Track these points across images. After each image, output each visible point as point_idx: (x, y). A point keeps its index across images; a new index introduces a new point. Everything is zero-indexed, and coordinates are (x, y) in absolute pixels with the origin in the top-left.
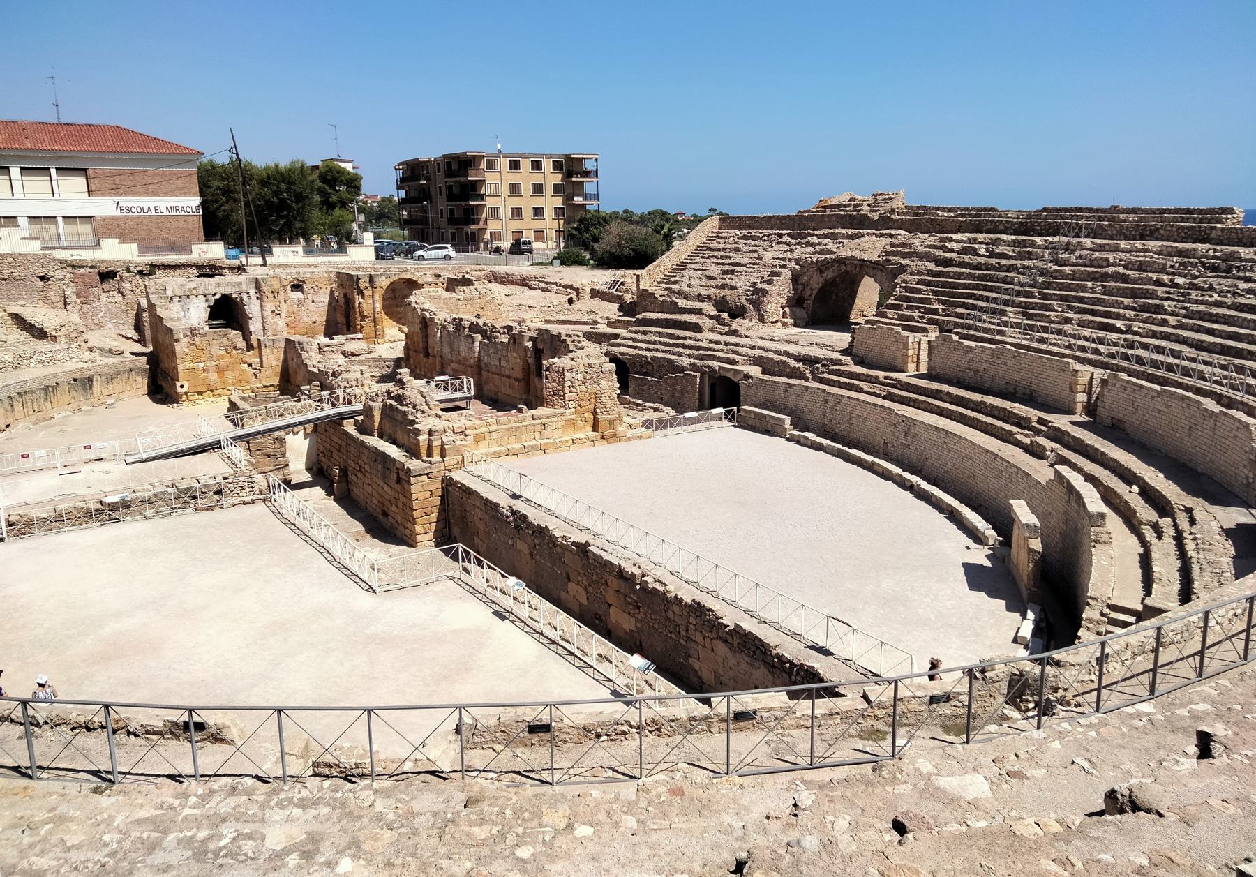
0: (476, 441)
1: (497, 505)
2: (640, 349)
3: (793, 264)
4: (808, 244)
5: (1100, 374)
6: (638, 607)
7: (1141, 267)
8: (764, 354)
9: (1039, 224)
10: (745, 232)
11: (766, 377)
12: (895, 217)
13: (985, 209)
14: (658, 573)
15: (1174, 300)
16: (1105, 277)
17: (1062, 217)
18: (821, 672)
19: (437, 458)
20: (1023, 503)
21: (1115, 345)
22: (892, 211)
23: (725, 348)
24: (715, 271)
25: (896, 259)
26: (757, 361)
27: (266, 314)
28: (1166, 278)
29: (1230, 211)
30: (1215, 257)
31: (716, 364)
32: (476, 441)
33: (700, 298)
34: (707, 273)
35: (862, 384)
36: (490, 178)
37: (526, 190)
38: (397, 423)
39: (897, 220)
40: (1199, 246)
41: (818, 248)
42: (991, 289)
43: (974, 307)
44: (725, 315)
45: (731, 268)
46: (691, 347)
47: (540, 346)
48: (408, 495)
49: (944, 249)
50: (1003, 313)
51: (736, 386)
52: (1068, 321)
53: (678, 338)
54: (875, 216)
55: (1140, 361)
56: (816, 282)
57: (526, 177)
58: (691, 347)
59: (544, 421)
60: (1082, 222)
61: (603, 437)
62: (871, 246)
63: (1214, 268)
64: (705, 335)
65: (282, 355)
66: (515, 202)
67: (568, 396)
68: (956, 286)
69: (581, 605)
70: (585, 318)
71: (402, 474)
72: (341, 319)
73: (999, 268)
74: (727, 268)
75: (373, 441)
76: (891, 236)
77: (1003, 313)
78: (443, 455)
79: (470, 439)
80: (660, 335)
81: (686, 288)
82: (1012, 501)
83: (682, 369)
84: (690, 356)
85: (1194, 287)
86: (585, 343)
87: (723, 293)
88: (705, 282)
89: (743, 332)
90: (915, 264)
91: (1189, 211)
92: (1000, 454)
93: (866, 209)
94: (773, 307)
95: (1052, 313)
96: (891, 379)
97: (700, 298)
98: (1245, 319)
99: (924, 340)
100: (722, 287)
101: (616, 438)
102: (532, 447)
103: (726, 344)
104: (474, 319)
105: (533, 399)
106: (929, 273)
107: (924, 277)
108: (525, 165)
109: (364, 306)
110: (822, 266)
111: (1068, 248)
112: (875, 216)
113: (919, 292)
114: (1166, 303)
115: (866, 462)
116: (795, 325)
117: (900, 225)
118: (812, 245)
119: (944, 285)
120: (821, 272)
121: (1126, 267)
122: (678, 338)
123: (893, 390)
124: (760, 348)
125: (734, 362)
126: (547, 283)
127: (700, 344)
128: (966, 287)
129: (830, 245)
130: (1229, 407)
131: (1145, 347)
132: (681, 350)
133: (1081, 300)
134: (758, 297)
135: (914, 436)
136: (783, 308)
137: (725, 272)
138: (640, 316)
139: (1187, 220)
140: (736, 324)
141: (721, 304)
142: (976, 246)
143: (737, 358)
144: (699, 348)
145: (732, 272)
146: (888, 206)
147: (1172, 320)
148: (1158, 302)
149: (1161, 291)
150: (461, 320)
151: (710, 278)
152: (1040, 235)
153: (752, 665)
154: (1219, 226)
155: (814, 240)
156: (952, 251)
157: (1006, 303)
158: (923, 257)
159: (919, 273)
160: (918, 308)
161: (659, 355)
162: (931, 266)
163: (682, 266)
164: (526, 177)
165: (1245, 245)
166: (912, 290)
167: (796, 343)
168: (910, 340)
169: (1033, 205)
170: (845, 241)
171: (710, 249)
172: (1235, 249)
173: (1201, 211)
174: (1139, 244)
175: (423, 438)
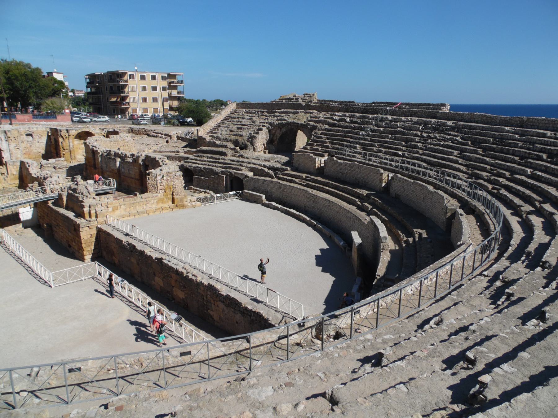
0: (113, 210)
1: (122, 241)
2: (198, 164)
3: (268, 125)
4: (275, 116)
5: (391, 175)
6: (185, 288)
8: (254, 166)
9: (371, 109)
10: (248, 110)
11: (255, 177)
12: (312, 104)
13: (350, 102)
14: (195, 272)
15: (422, 143)
17: (381, 106)
18: (264, 315)
19: (93, 218)
20: (357, 233)
21: (398, 162)
23: (237, 163)
24: (234, 128)
25: (312, 123)
26: (252, 170)
27: (11, 148)
28: (419, 133)
29: (444, 105)
31: (233, 171)
32: (113, 210)
33: (227, 140)
34: (230, 128)
35: (297, 180)
36: (131, 83)
37: (149, 89)
38: (74, 203)
39: (313, 106)
40: (433, 121)
42: (351, 137)
43: (343, 145)
44: (238, 148)
45: (241, 126)
47: (147, 164)
48: (79, 236)
51: (241, 181)
52: (381, 151)
53: (216, 159)
54: (304, 104)
55: (407, 169)
56: (278, 133)
57: (149, 83)
59: (147, 199)
60: (388, 108)
61: (177, 206)
62: (302, 118)
64: (229, 157)
65: (18, 169)
66: (144, 95)
67: (159, 187)
68: (337, 136)
69: (161, 287)
70: (173, 150)
71: (76, 227)
72: (53, 150)
73: (355, 128)
74: (239, 126)
75: (62, 211)
76: (310, 113)
77: (355, 148)
78: (97, 217)
79: (110, 209)
80: (208, 157)
81: (220, 136)
82: (352, 232)
83: (217, 173)
84: (221, 167)
86: (168, 161)
87: (237, 138)
88: (228, 132)
89: (246, 155)
90: (319, 126)
91: (429, 105)
92: (350, 211)
93: (300, 100)
95: (375, 148)
96: (308, 177)
97: (227, 140)
98: (447, 151)
99: (323, 159)
100: (236, 135)
101: (184, 206)
102: (142, 213)
103: (238, 161)
104: (117, 151)
105: (144, 189)
106: (326, 130)
108: (148, 76)
109: (64, 144)
110: (281, 126)
111: (382, 120)
112: (304, 104)
113: (321, 138)
114: (419, 144)
115: (297, 215)
116: (269, 153)
117: (314, 108)
118: (277, 117)
119: (332, 135)
120: (281, 129)
122: (216, 159)
123: (309, 182)
124: (253, 163)
125: (241, 170)
126: (157, 133)
127: (226, 161)
128: (341, 136)
129: (284, 116)
130: (438, 189)
131: (409, 163)
132: (217, 165)
133: (386, 142)
134: (252, 139)
135: (317, 203)
136: (264, 144)
137: (238, 128)
138: (199, 149)
140: (243, 152)
143: (242, 168)
144: (226, 164)
145: (241, 128)
146: (309, 100)
147: (421, 151)
148: (416, 144)
149: (417, 139)
150: (110, 151)
151: (231, 131)
152: (372, 114)
153: (235, 313)
155: (277, 114)
157: (357, 143)
159: (323, 130)
160: (320, 145)
161: (207, 167)
162: (327, 127)
163: (219, 125)
164: (149, 83)
165: (449, 120)
166: (318, 137)
167: (268, 161)
168: (317, 160)
169: (369, 101)
170: (291, 115)
171: (232, 118)
172: (446, 121)
173: (434, 105)
175: (86, 210)
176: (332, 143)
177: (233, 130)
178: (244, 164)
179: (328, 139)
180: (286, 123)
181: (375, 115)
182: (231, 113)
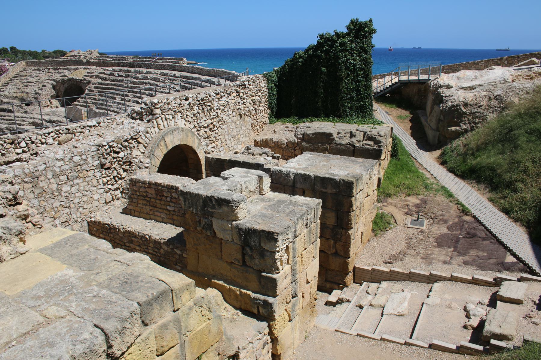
3: (52, 82)
4: (59, 73)
7: (155, 79)
10: (36, 68)
12: (92, 61)
16: (146, 83)
17: (143, 61)
22: (91, 58)
24: (20, 85)
30: (172, 76)
33: (14, 98)
39: (92, 63)
41: (63, 74)
45: (28, 84)
46: (7, 120)
49: (104, 73)
50: (115, 99)
52: (129, 101)
54: (85, 60)
56: (62, 89)
58: (7, 120)
63: (170, 80)
74: (26, 84)
77: (115, 99)
81: (7, 94)
85: (163, 87)
88: (16, 90)
94: (44, 101)
97: (14, 98)
103: (22, 117)
106: (99, 84)
107: (97, 86)
110: (63, 82)
111: (139, 72)
112: (85, 60)
113: (93, 91)
121: (151, 79)
124: (34, 118)
127: (11, 118)
129: (66, 73)
133: (136, 92)
137: (26, 86)
139: (172, 62)
140: (28, 109)
141: (22, 100)
142: (114, 72)
143: (24, 123)
144: (10, 120)
151: (19, 89)
154: (177, 65)
156: (107, 74)
157: (117, 94)
158: (97, 76)
159: (95, 84)
174: (156, 71)
176: (100, 95)
177: (19, 87)
178: (27, 120)
179: (99, 92)
180: (67, 80)
181: (136, 69)
182: (21, 71)
